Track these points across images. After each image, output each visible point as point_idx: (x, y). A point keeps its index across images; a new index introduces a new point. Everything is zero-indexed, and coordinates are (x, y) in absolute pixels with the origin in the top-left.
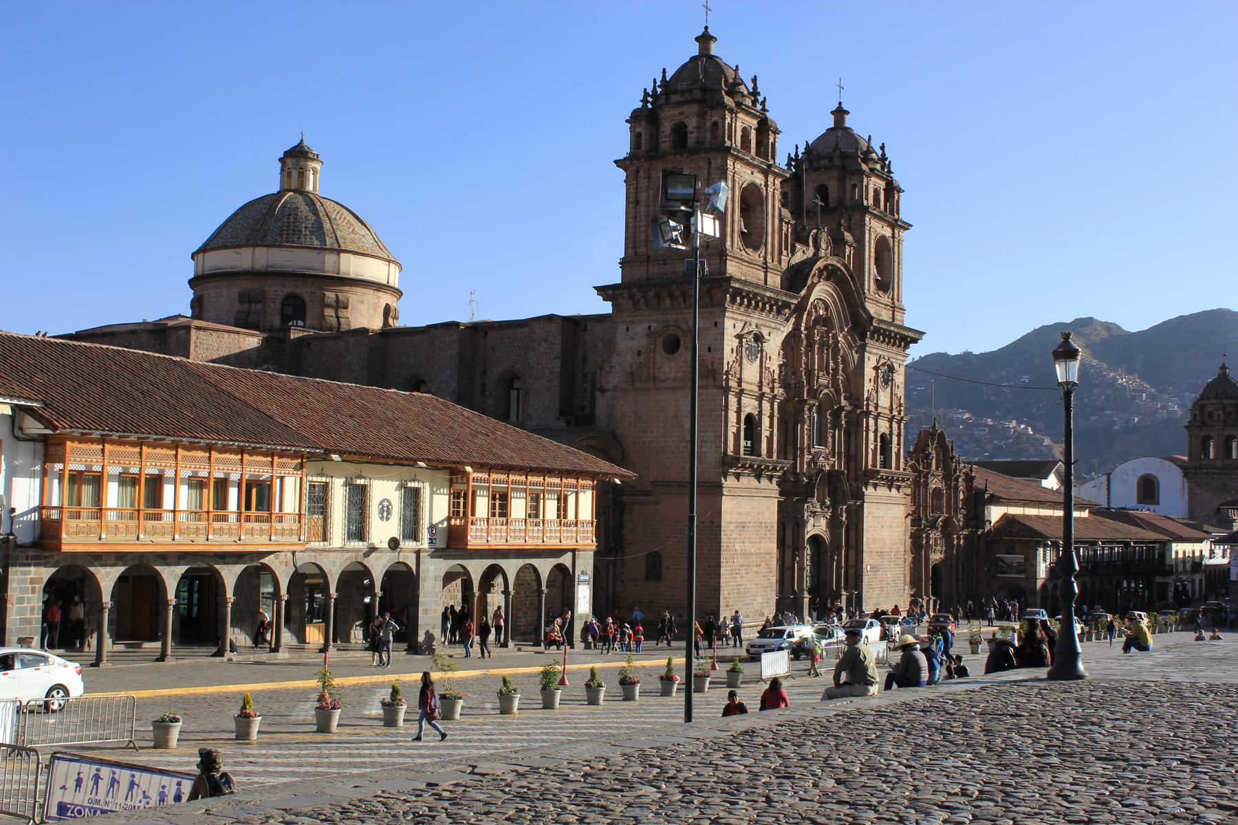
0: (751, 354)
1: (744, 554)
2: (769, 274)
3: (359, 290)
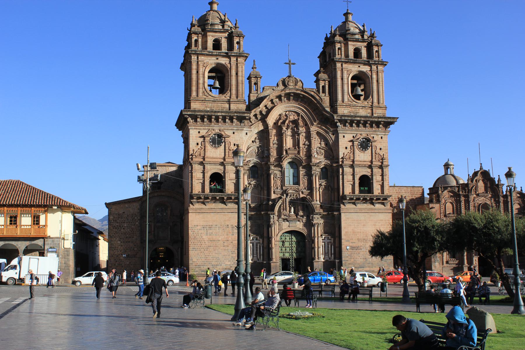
1: (211, 241)
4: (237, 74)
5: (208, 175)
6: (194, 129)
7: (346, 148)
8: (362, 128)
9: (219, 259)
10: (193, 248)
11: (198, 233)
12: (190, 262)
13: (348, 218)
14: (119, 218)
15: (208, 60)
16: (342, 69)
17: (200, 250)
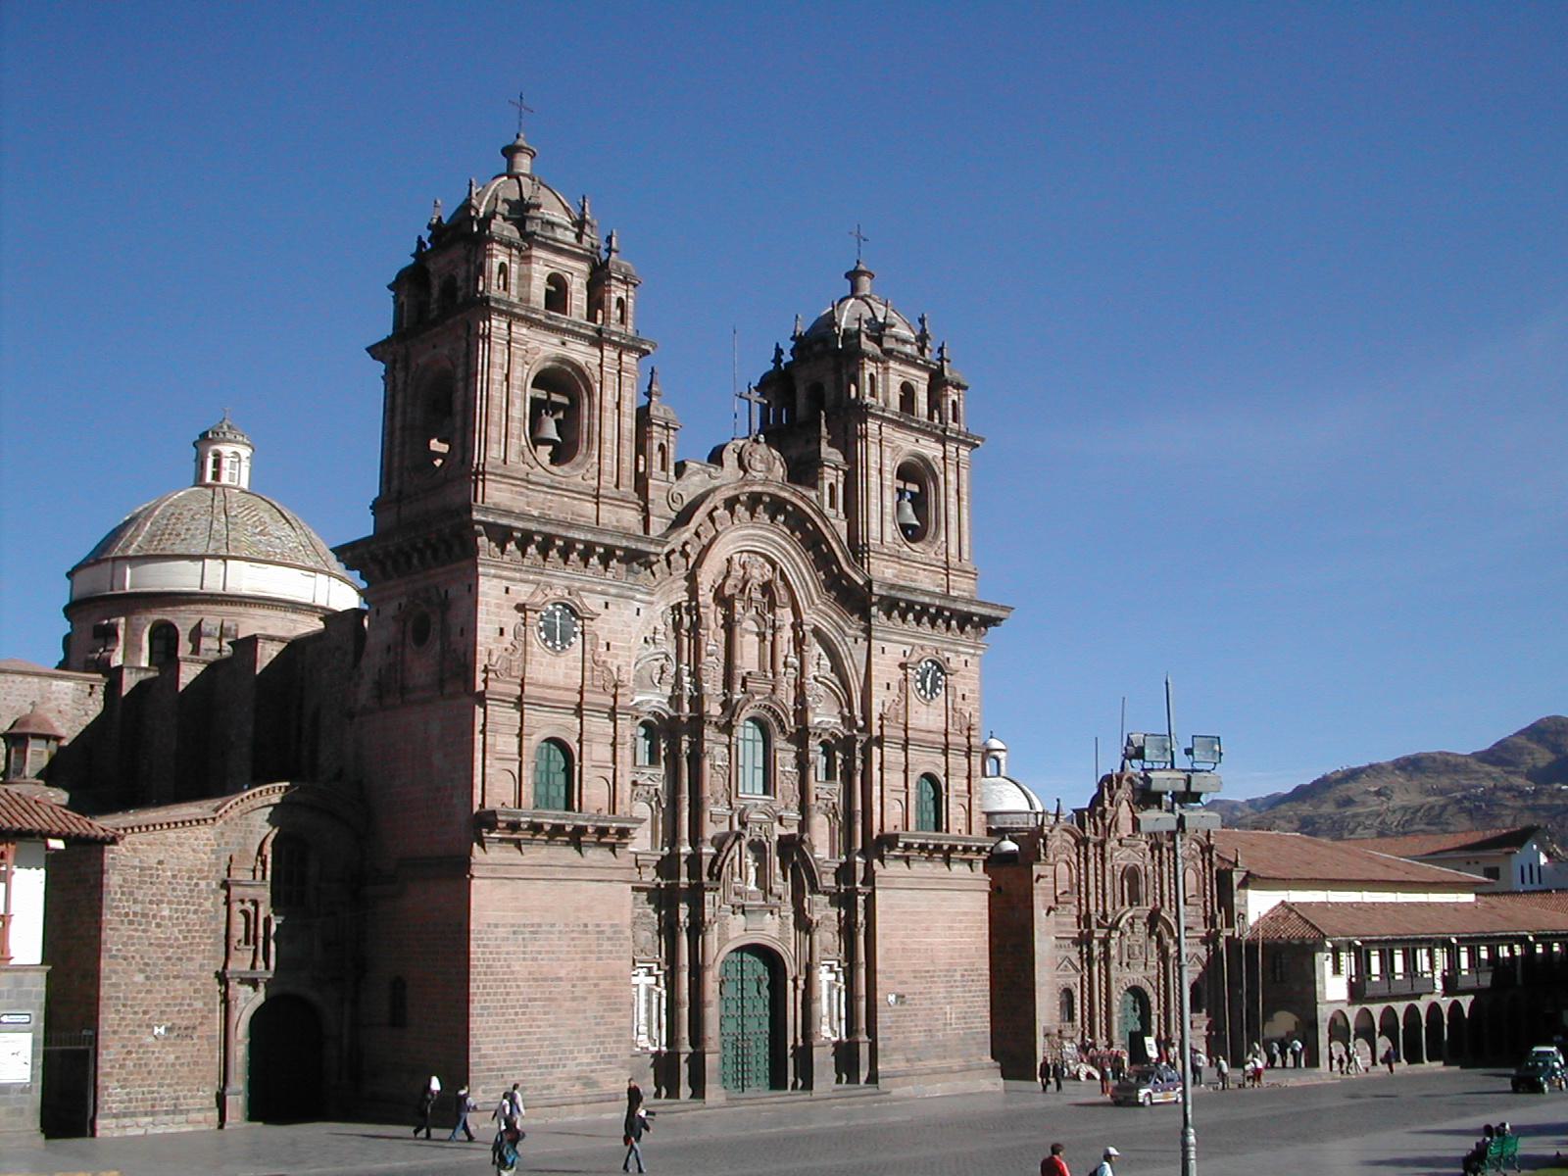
0: (551, 636)
2: (601, 505)
3: (252, 611)
5: (532, 742)
6: (495, 576)
8: (926, 627)
9: (555, 1046)
10: (482, 1008)
11: (497, 953)
12: (473, 1057)
13: (891, 907)
14: (145, 882)
15: (537, 344)
16: (881, 441)
17: (503, 1014)
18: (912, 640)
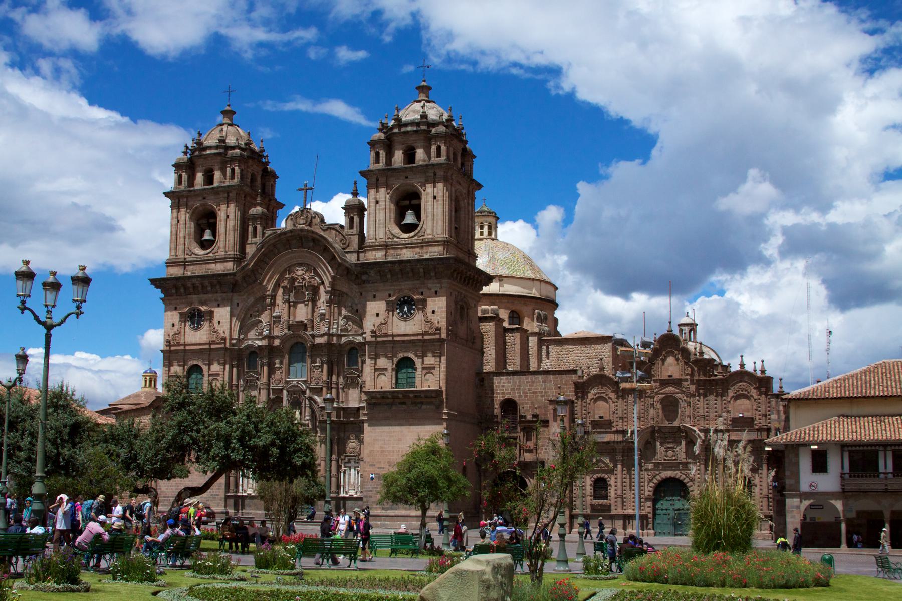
4: (228, 217)
7: (378, 315)
18: (393, 288)
